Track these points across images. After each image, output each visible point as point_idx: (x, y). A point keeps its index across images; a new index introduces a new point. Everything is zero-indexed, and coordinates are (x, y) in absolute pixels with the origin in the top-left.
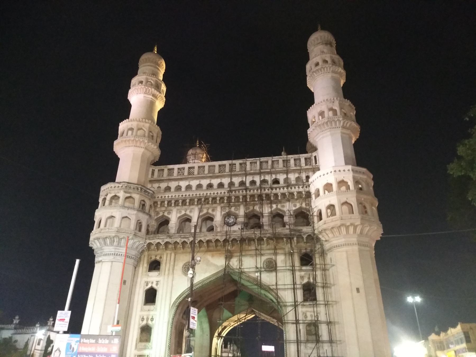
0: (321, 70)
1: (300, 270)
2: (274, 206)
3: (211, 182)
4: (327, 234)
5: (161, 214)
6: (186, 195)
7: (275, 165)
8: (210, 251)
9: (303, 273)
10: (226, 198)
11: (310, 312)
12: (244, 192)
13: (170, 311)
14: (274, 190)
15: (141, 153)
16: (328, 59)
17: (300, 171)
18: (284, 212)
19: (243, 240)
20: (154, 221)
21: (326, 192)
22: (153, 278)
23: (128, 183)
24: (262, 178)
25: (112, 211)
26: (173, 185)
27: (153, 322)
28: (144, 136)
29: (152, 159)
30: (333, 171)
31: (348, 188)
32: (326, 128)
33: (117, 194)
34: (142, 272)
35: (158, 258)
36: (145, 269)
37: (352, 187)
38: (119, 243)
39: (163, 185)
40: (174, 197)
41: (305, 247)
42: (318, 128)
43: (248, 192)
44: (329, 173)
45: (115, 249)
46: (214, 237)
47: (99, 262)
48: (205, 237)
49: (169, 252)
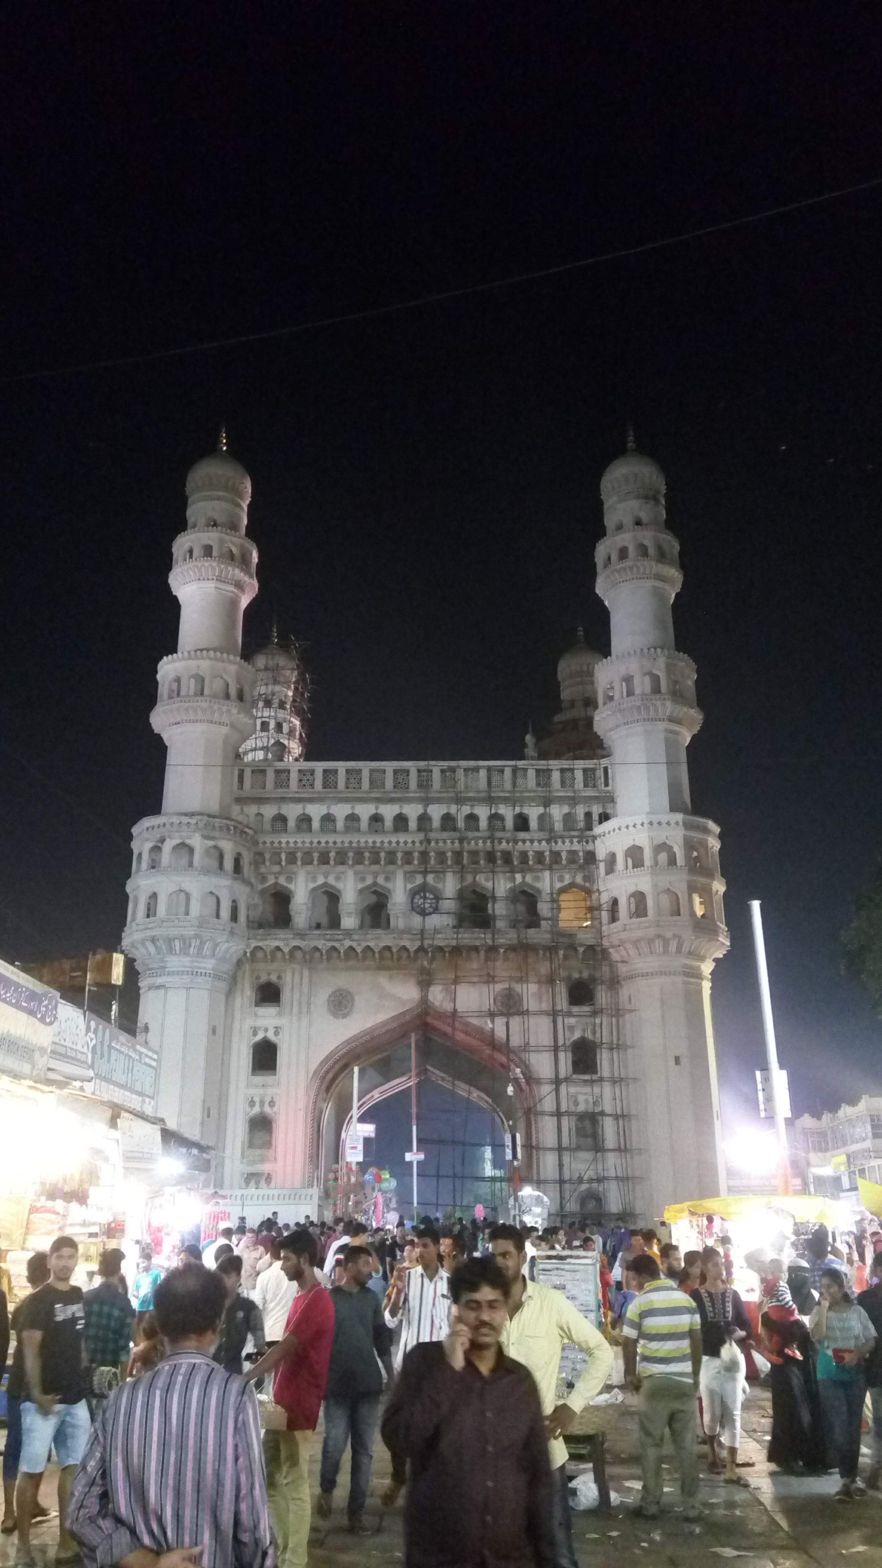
0: (631, 568)
1: (570, 1014)
2: (518, 877)
3: (379, 811)
4: (626, 949)
5: (271, 881)
6: (327, 842)
7: (520, 781)
8: (388, 968)
9: (572, 1021)
10: (416, 854)
11: (585, 1094)
12: (457, 844)
13: (308, 1089)
14: (520, 843)
16: (644, 516)
17: (573, 801)
18: (539, 891)
19: (457, 950)
21: (630, 861)
22: (267, 1021)
24: (493, 812)
26: (292, 811)
27: (275, 1109)
28: (227, 697)
30: (646, 822)
31: (672, 861)
33: (188, 841)
35: (274, 978)
37: (680, 860)
38: (200, 948)
39: (269, 811)
40: (300, 845)
41: (579, 971)
42: (619, 716)
43: (465, 844)
44: (639, 827)
47: (159, 987)
49: (297, 967)
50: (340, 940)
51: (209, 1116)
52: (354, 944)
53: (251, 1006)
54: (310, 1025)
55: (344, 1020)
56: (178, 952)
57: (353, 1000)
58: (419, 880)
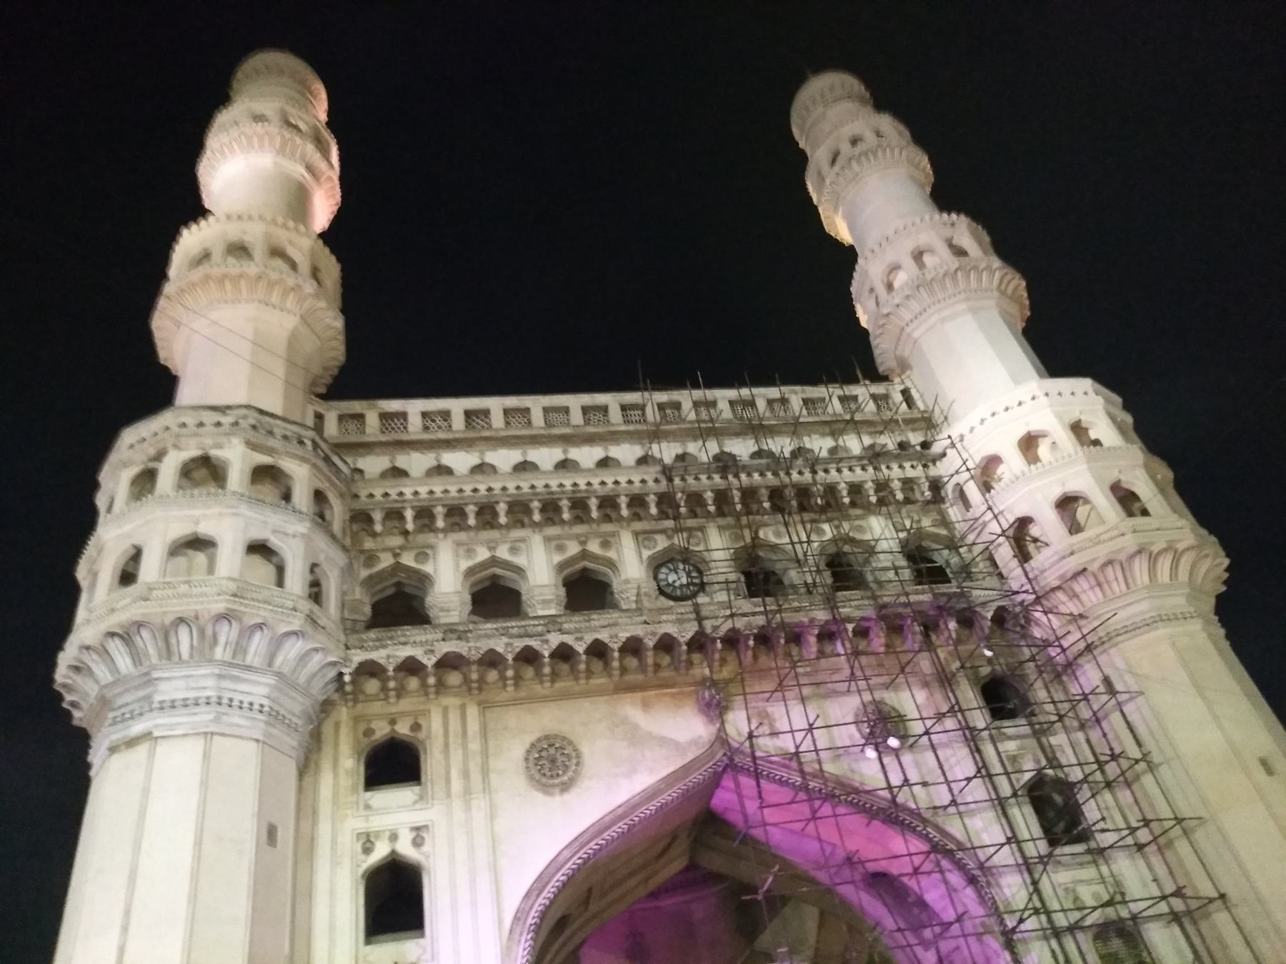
2: (828, 531)
5: (386, 561)
8: (632, 688)
9: (1010, 747)
11: (1089, 882)
19: (764, 639)
20: (358, 590)
22: (395, 816)
23: (261, 412)
25: (196, 513)
32: (951, 290)
33: (214, 453)
34: (336, 795)
35: (403, 729)
36: (345, 782)
38: (240, 648)
45: (220, 676)
46: (649, 628)
47: (131, 743)
48: (614, 630)
49: (451, 701)
52: (569, 639)
53: (354, 789)
54: (492, 817)
55: (567, 796)
56: (185, 656)
57: (578, 756)
58: (662, 543)
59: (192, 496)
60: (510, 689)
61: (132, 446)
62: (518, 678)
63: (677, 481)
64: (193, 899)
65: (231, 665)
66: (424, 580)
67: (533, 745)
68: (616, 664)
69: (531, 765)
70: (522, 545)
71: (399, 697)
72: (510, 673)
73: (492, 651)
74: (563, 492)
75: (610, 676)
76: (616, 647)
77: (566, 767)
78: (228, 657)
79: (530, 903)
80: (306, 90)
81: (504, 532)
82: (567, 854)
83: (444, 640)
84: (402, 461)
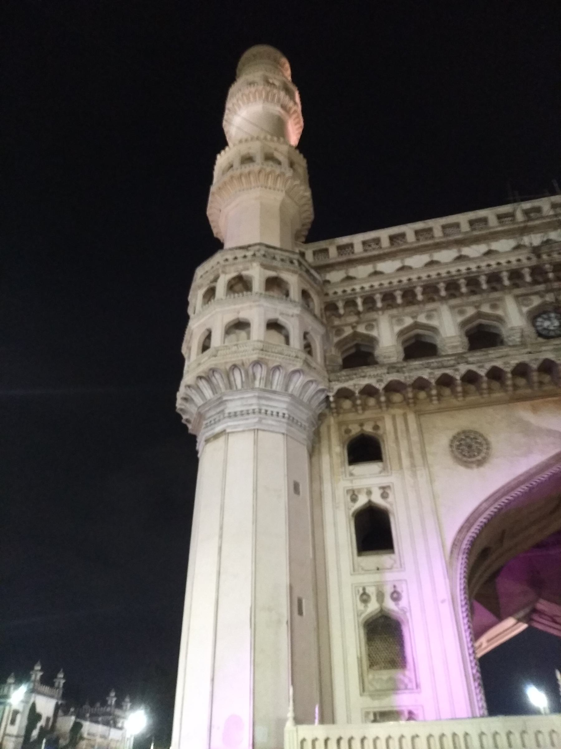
5: (348, 331)
13: (450, 566)
15: (278, 204)
20: (333, 349)
22: (368, 480)
23: (268, 247)
25: (238, 307)
29: (298, 227)
33: (244, 273)
34: (332, 467)
35: (368, 429)
36: (337, 460)
38: (268, 381)
45: (259, 398)
47: (216, 436)
48: (506, 359)
49: (398, 412)
50: (452, 366)
51: (300, 613)
52: (473, 368)
53: (342, 464)
54: (431, 481)
55: (482, 469)
56: (239, 386)
57: (488, 443)
58: (536, 301)
59: (234, 297)
60: (435, 402)
61: (201, 277)
62: (440, 396)
63: (545, 257)
64: (255, 521)
65: (264, 390)
66: (372, 341)
67: (454, 437)
68: (509, 382)
69: (454, 449)
70: (434, 313)
71: (364, 409)
72: (434, 392)
73: (420, 379)
74: (460, 275)
75: (506, 391)
76: (508, 370)
77: (479, 451)
78: (262, 386)
79: (462, 536)
80: (276, 62)
81: (421, 306)
82: (485, 505)
83: (388, 373)
84: (352, 272)
